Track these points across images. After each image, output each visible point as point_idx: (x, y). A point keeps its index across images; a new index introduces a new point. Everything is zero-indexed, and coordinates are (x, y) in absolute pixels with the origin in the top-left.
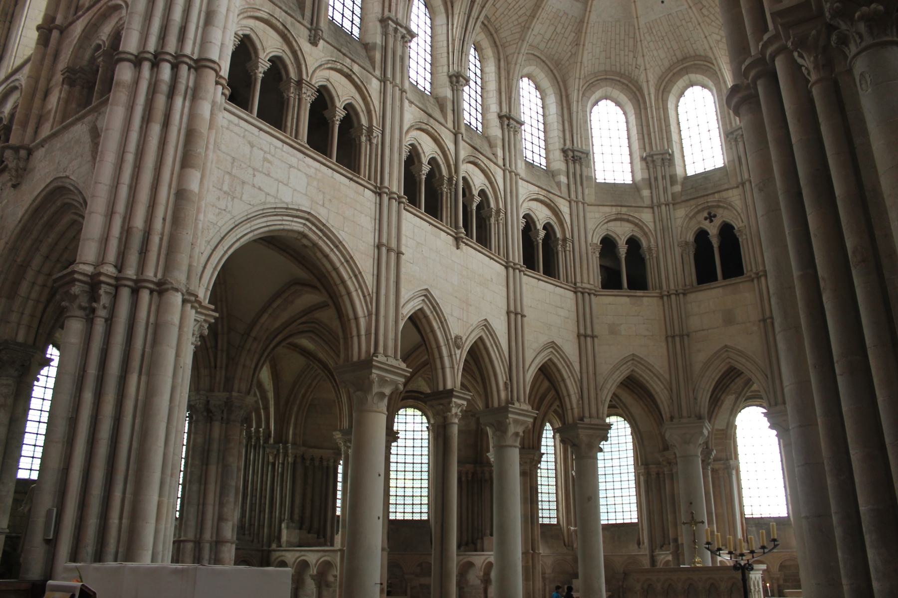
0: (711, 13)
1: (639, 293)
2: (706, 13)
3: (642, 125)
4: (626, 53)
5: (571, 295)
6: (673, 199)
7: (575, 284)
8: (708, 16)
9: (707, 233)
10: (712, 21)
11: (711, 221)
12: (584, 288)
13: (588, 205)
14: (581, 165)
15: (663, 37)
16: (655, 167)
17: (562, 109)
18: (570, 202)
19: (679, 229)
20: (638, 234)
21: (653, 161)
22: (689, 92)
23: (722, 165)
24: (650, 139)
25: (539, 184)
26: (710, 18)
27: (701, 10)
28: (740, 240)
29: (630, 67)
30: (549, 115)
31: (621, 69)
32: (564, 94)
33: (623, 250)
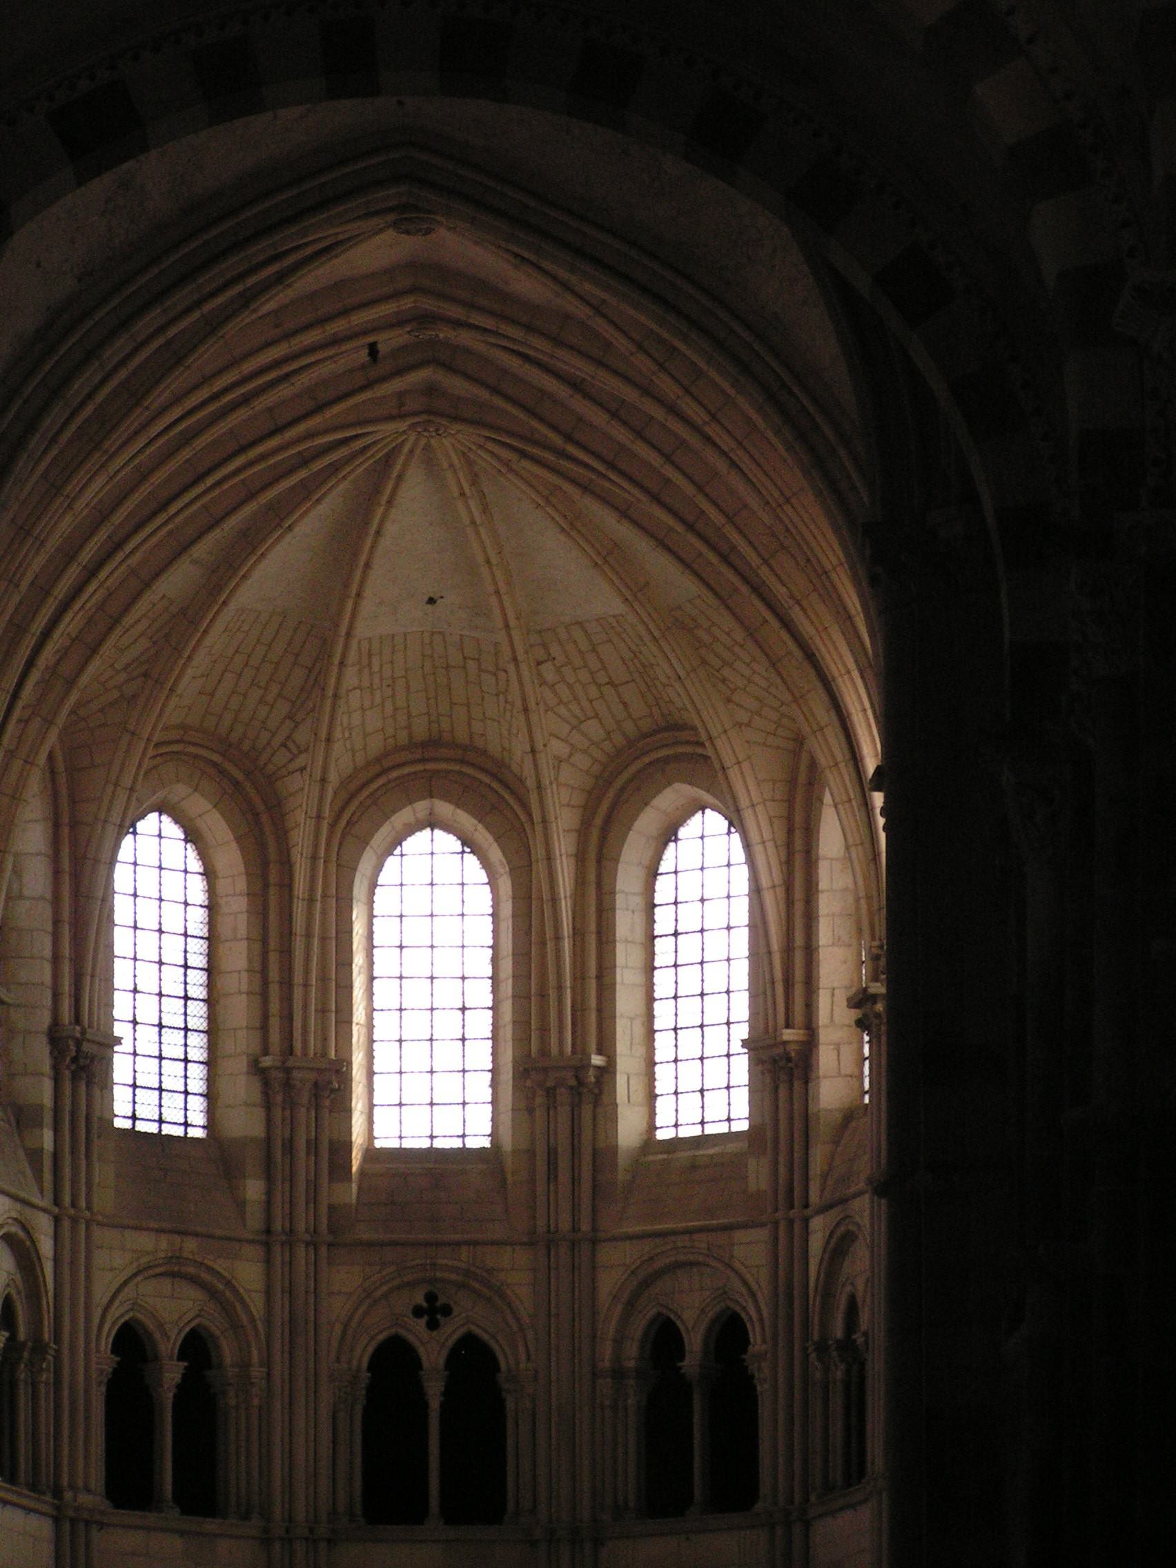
0: (563, 680)
1: (211, 1525)
2: (550, 676)
3: (265, 941)
4: (270, 698)
5: (42, 1527)
6: (331, 1231)
7: (57, 1492)
8: (552, 687)
9: (417, 1363)
10: (561, 702)
11: (433, 1325)
12: (76, 1509)
13: (99, 1224)
14: (89, 1084)
15: (393, 678)
16: (291, 1104)
17: (57, 873)
18: (57, 1220)
19: (338, 1329)
20: (215, 1324)
21: (288, 1085)
22: (419, 842)
23: (486, 1143)
24: (287, 999)
25: (13, 1190)
26: (556, 694)
27: (539, 663)
28: (510, 1405)
29: (265, 736)
30: (21, 897)
31: (231, 730)
32: (65, 819)
33: (172, 1374)
